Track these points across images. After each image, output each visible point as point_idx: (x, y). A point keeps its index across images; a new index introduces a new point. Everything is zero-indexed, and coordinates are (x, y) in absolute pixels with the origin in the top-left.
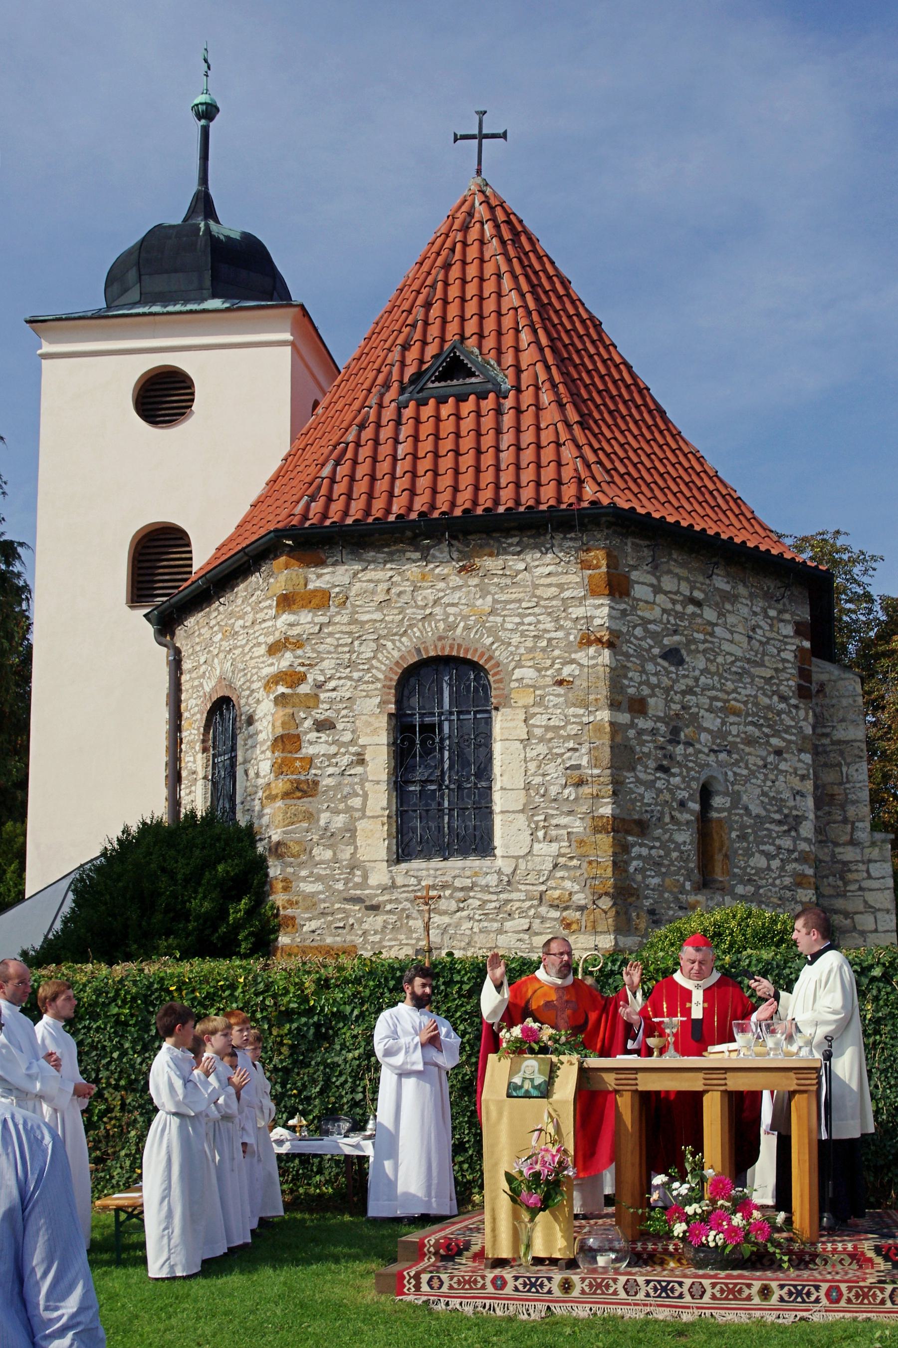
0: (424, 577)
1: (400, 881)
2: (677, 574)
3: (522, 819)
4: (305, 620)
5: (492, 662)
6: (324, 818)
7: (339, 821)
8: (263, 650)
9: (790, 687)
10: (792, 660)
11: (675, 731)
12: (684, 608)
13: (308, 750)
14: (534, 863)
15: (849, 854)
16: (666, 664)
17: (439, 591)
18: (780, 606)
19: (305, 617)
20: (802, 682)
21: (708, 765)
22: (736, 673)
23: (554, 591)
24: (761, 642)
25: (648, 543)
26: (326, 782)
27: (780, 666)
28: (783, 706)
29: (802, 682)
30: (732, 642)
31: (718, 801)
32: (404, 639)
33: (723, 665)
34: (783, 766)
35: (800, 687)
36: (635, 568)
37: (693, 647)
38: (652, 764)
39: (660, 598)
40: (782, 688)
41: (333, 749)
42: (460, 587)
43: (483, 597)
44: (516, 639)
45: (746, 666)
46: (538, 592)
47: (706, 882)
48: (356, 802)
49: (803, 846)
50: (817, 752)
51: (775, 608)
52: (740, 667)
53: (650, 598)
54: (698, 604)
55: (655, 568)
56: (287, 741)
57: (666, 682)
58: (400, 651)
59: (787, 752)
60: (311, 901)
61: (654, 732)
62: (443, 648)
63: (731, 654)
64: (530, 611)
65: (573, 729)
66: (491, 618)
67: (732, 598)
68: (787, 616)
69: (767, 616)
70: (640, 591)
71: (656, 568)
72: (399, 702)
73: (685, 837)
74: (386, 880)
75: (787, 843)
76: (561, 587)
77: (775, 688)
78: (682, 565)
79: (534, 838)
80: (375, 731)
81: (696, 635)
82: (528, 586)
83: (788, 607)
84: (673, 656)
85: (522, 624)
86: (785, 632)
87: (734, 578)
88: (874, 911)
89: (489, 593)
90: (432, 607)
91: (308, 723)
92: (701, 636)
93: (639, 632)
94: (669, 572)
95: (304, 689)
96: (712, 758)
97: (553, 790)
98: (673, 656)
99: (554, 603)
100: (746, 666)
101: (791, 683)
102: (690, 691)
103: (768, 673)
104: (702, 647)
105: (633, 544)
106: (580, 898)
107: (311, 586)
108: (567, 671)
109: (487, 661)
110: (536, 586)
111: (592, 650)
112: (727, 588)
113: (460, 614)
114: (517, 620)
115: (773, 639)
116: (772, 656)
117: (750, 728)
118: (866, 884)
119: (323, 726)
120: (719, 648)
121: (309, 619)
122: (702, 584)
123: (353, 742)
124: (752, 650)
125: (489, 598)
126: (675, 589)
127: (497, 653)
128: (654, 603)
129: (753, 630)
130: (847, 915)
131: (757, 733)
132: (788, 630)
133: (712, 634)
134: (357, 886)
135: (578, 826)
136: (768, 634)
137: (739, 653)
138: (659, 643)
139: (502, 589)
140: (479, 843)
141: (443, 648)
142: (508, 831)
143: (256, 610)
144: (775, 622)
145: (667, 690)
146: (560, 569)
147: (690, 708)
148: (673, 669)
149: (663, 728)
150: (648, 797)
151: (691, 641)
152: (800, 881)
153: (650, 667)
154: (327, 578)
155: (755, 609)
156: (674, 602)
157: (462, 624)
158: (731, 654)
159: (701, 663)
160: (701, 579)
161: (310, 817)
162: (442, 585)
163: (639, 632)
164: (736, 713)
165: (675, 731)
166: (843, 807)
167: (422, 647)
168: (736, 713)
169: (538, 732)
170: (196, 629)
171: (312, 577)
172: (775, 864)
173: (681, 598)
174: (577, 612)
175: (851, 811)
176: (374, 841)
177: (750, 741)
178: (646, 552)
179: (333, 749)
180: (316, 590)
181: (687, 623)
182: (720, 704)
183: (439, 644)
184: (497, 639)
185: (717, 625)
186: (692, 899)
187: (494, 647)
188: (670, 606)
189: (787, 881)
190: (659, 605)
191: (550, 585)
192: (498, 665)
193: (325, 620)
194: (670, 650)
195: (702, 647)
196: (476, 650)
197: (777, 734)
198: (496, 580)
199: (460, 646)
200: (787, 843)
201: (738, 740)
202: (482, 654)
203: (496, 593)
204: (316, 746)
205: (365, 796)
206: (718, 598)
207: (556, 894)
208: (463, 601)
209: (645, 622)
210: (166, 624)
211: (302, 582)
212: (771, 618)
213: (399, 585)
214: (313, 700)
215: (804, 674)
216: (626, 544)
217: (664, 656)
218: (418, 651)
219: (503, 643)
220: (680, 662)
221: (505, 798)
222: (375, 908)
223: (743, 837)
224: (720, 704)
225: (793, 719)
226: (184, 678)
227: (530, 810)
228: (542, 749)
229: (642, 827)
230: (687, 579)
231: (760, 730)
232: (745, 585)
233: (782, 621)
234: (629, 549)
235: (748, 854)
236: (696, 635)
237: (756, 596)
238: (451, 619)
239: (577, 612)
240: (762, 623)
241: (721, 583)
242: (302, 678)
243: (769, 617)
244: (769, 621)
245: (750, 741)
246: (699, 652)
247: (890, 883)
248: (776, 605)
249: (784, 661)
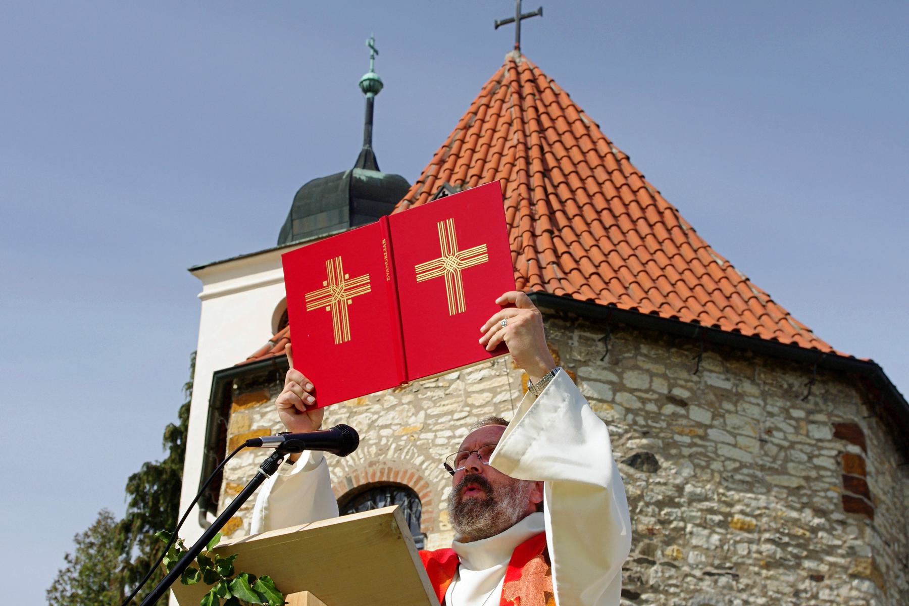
2: (648, 371)
5: (422, 483)
9: (830, 499)
10: (833, 467)
12: (660, 408)
16: (631, 471)
17: (374, 413)
18: (810, 406)
20: (849, 493)
21: (699, 591)
22: (743, 482)
23: (487, 396)
24: (781, 447)
25: (601, 336)
27: (813, 474)
28: (817, 521)
29: (849, 493)
30: (735, 446)
32: (338, 470)
33: (720, 472)
35: (846, 500)
36: (585, 363)
37: (673, 451)
40: (816, 499)
42: (393, 407)
43: (415, 414)
45: (759, 474)
46: (470, 401)
51: (802, 409)
52: (748, 475)
53: (609, 396)
54: (682, 403)
59: (830, 577)
62: (374, 474)
63: (734, 460)
64: (462, 422)
66: (423, 436)
67: (739, 397)
68: (821, 417)
69: (790, 417)
71: (616, 362)
76: (494, 391)
77: (805, 500)
78: (656, 361)
81: (677, 438)
82: (460, 396)
83: (823, 407)
85: (454, 437)
86: (817, 435)
87: (735, 374)
89: (422, 408)
90: (367, 432)
92: (687, 440)
94: (636, 367)
99: (486, 410)
100: (759, 474)
101: (830, 494)
102: (669, 502)
103: (794, 483)
104: (686, 451)
105: (580, 337)
107: (255, 427)
109: (416, 483)
110: (468, 394)
112: (727, 385)
113: (393, 435)
114: (449, 433)
115: (800, 443)
116: (800, 463)
120: (715, 452)
121: (250, 461)
122: (687, 381)
124: (766, 455)
125: (422, 414)
126: (646, 386)
127: (427, 473)
128: (613, 401)
129: (769, 432)
131: (779, 554)
132: (826, 433)
133: (704, 438)
136: (792, 438)
137: (747, 458)
139: (435, 402)
141: (374, 474)
144: (803, 424)
146: (493, 373)
147: (671, 522)
148: (643, 476)
151: (668, 445)
154: (269, 416)
155: (769, 408)
156: (644, 401)
157: (394, 446)
158: (734, 460)
160: (685, 375)
162: (377, 407)
167: (353, 476)
171: (257, 417)
173: (655, 396)
178: (600, 346)
181: (664, 425)
182: (717, 518)
183: (370, 471)
184: (428, 457)
185: (711, 426)
187: (424, 466)
188: (637, 405)
190: (620, 404)
191: (482, 391)
192: (427, 485)
194: (637, 456)
195: (686, 451)
196: (406, 472)
197: (814, 555)
198: (429, 394)
199: (390, 469)
201: (750, 561)
202: (412, 475)
203: (429, 408)
206: (712, 397)
208: (396, 421)
211: (247, 423)
212: (797, 420)
213: (336, 413)
216: (571, 338)
218: (349, 480)
219: (434, 460)
224: (717, 518)
225: (838, 537)
230: (664, 376)
231: (784, 550)
232: (753, 382)
233: (813, 422)
234: (575, 342)
236: (677, 438)
237: (772, 395)
238: (384, 441)
240: (782, 425)
243: (792, 418)
244: (793, 422)
246: (684, 457)
248: (804, 405)
249: (818, 468)
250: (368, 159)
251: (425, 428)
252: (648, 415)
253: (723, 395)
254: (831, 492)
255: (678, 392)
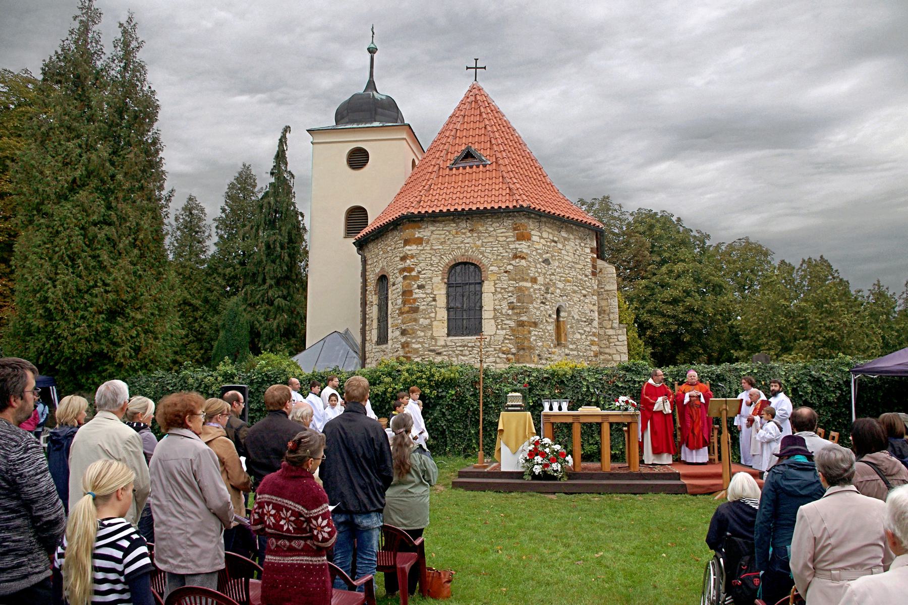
0: (457, 233)
1: (449, 344)
3: (493, 321)
4: (412, 249)
6: (421, 321)
7: (428, 321)
8: (398, 259)
11: (547, 289)
13: (415, 296)
14: (497, 337)
15: (611, 332)
19: (414, 247)
26: (421, 307)
31: (562, 314)
34: (586, 301)
38: (539, 301)
39: (542, 240)
41: (424, 296)
44: (490, 256)
47: (559, 344)
48: (433, 315)
49: (594, 330)
50: (599, 294)
54: (556, 242)
55: (540, 230)
56: (406, 293)
57: (544, 271)
58: (447, 260)
60: (416, 351)
61: (540, 289)
65: (511, 289)
70: (535, 238)
72: (448, 278)
73: (551, 328)
74: (443, 343)
75: (588, 329)
76: (506, 237)
79: (497, 329)
80: (439, 289)
84: (546, 261)
88: (620, 353)
91: (416, 286)
93: (534, 253)
95: (414, 274)
96: (560, 299)
97: (504, 311)
98: (546, 261)
102: (553, 274)
103: (581, 267)
106: (514, 350)
108: (510, 267)
111: (517, 260)
117: (575, 288)
118: (617, 343)
119: (421, 287)
123: (432, 293)
130: (610, 354)
132: (588, 250)
134: (433, 346)
135: (512, 324)
138: (541, 257)
140: (476, 329)
142: (488, 327)
143: (396, 243)
145: (545, 274)
149: (543, 288)
150: (538, 313)
151: (553, 256)
152: (593, 343)
153: (538, 266)
159: (557, 264)
161: (416, 320)
163: (534, 253)
164: (569, 282)
165: (547, 289)
166: (608, 315)
168: (569, 282)
169: (498, 290)
170: (376, 251)
172: (584, 337)
174: (512, 246)
175: (612, 316)
176: (440, 329)
177: (575, 292)
178: (537, 224)
179: (424, 296)
180: (418, 238)
186: (554, 350)
189: (588, 343)
193: (420, 248)
197: (584, 289)
200: (588, 329)
204: (418, 294)
205: (436, 313)
207: (504, 349)
209: (537, 249)
210: (361, 245)
214: (416, 278)
215: (594, 267)
217: (543, 262)
220: (549, 264)
221: (487, 314)
222: (439, 354)
223: (571, 327)
226: (368, 267)
227: (495, 318)
228: (500, 296)
229: (535, 324)
235: (574, 333)
239: (512, 246)
241: (564, 234)
242: (413, 270)
245: (575, 292)
247: (626, 343)
250: (371, 85)
251: (482, 246)
252: (549, 247)
253: (565, 239)
254: (589, 271)
255: (556, 239)
